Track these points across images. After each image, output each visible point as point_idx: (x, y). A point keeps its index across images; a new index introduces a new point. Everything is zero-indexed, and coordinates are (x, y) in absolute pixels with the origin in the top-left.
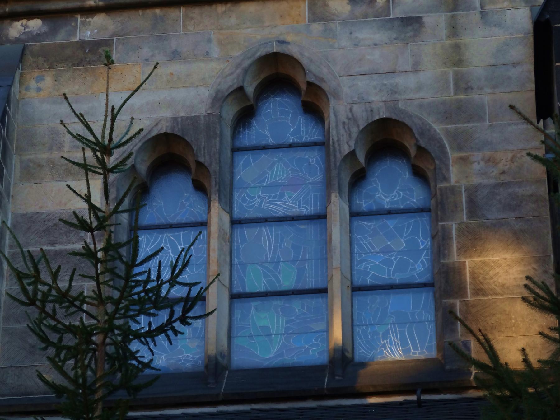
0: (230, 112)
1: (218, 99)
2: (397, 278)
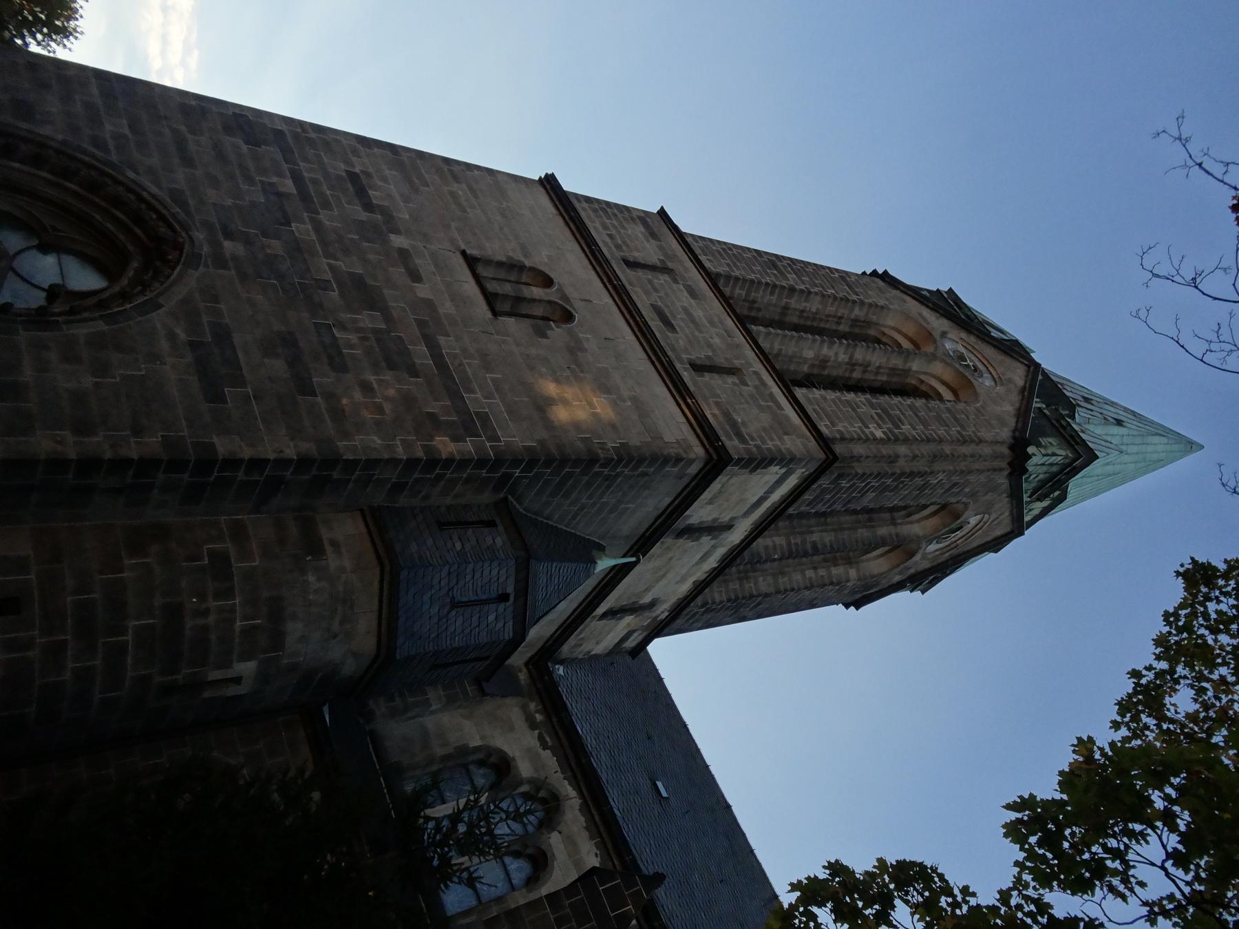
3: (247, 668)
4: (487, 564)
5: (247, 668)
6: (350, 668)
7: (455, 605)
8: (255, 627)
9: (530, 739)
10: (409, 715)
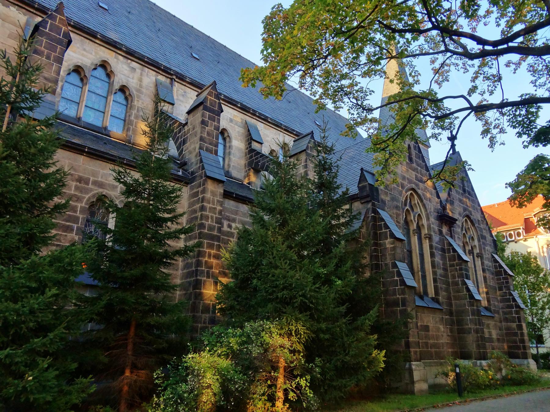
0: (93, 67)
1: (92, 64)
2: (118, 116)
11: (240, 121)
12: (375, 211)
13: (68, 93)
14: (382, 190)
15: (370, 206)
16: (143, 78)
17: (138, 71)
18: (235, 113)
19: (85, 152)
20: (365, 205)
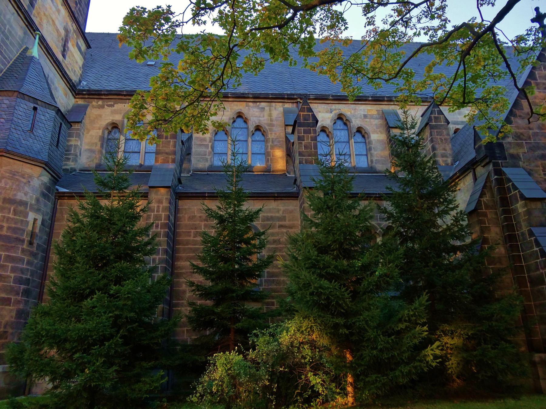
0: (232, 121)
1: (230, 119)
2: (259, 152)
3: (31, 216)
4: (16, 111)
5: (31, 216)
6: (46, 178)
7: (32, 130)
8: (14, 210)
9: (107, 110)
10: (78, 154)
11: (376, 113)
12: (498, 172)
13: (218, 149)
14: (510, 143)
15: (491, 167)
16: (272, 112)
17: (267, 109)
18: (369, 107)
19: (206, 197)
20: (486, 167)
